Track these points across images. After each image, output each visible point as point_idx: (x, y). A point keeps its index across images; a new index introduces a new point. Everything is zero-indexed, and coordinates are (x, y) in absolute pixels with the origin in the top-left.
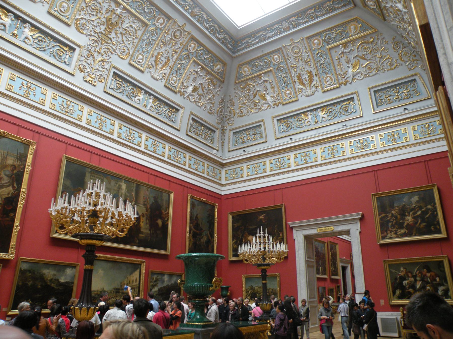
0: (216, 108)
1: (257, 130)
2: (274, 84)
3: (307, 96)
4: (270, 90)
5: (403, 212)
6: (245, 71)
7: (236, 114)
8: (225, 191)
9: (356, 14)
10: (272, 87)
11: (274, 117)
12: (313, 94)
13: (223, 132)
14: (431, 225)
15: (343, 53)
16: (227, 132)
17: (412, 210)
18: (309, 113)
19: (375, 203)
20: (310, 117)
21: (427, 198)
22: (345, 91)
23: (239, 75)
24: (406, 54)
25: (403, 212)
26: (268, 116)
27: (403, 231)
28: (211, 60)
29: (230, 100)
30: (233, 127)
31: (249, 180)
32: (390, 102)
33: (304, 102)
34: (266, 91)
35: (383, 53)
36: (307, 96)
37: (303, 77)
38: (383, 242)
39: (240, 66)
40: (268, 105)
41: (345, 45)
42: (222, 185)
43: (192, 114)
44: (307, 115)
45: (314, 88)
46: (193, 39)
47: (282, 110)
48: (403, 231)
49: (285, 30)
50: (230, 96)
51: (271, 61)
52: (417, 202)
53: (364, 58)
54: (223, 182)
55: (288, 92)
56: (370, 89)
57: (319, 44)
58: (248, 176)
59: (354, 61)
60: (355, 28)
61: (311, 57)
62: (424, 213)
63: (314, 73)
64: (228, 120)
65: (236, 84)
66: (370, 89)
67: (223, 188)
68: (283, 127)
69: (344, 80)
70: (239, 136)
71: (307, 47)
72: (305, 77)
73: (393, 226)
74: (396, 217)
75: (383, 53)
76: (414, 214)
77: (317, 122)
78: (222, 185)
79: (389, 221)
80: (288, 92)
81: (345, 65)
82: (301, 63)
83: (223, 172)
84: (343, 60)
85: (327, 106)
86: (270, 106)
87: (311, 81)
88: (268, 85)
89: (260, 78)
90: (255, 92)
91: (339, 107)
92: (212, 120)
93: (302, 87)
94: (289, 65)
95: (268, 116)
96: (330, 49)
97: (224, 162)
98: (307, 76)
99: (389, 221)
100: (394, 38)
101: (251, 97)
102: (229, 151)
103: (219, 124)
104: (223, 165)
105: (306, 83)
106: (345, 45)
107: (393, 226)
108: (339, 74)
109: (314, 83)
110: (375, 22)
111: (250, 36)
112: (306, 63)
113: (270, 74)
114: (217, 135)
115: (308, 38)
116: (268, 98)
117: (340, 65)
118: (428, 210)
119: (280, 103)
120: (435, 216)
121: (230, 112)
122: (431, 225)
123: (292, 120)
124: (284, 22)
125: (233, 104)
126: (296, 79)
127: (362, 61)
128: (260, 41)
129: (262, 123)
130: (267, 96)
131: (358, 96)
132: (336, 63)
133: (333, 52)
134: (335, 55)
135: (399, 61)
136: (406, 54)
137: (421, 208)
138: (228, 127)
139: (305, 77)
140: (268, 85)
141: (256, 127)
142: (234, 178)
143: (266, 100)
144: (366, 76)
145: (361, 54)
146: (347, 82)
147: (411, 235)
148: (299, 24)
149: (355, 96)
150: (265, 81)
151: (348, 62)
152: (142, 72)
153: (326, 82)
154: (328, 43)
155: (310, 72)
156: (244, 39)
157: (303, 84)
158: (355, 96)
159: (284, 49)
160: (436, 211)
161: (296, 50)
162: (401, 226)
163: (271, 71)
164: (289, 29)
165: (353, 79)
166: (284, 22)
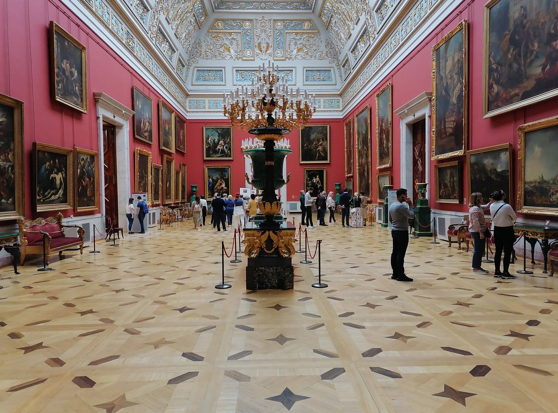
0: (190, 49)
2: (239, 42)
3: (261, 59)
7: (202, 56)
8: (189, 116)
15: (294, 39)
16: (192, 68)
22: (287, 64)
23: (213, 27)
24: (330, 53)
26: (229, 64)
30: (197, 65)
36: (261, 59)
37: (262, 45)
41: (297, 34)
42: (187, 112)
43: (180, 55)
45: (268, 56)
47: (240, 64)
49: (261, 8)
50: (200, 39)
58: (210, 108)
59: (299, 47)
61: (272, 33)
63: (270, 45)
64: (194, 58)
65: (208, 32)
67: (188, 114)
71: (272, 26)
72: (264, 45)
78: (187, 112)
81: (293, 46)
82: (263, 35)
83: (187, 101)
84: (292, 43)
88: (235, 42)
90: (223, 44)
92: (186, 57)
93: (260, 52)
94: (255, 33)
95: (229, 64)
97: (189, 93)
98: (265, 45)
100: (327, 40)
104: (188, 95)
105: (263, 49)
109: (269, 52)
110: (322, 29)
112: (269, 36)
113: (239, 34)
116: (232, 51)
117: (289, 45)
119: (240, 58)
123: (247, 73)
124: (263, 3)
125: (200, 46)
126: (257, 45)
128: (239, 9)
129: (223, 69)
130: (231, 49)
132: (288, 43)
133: (288, 35)
134: (289, 38)
138: (194, 65)
139: (264, 45)
140: (235, 42)
141: (219, 71)
143: (230, 52)
145: (304, 43)
146: (290, 58)
149: (294, 69)
150: (233, 39)
152: (169, 23)
153: (277, 53)
155: (268, 44)
158: (294, 69)
159: (255, 21)
164: (265, 8)
165: (295, 58)
166: (263, 3)
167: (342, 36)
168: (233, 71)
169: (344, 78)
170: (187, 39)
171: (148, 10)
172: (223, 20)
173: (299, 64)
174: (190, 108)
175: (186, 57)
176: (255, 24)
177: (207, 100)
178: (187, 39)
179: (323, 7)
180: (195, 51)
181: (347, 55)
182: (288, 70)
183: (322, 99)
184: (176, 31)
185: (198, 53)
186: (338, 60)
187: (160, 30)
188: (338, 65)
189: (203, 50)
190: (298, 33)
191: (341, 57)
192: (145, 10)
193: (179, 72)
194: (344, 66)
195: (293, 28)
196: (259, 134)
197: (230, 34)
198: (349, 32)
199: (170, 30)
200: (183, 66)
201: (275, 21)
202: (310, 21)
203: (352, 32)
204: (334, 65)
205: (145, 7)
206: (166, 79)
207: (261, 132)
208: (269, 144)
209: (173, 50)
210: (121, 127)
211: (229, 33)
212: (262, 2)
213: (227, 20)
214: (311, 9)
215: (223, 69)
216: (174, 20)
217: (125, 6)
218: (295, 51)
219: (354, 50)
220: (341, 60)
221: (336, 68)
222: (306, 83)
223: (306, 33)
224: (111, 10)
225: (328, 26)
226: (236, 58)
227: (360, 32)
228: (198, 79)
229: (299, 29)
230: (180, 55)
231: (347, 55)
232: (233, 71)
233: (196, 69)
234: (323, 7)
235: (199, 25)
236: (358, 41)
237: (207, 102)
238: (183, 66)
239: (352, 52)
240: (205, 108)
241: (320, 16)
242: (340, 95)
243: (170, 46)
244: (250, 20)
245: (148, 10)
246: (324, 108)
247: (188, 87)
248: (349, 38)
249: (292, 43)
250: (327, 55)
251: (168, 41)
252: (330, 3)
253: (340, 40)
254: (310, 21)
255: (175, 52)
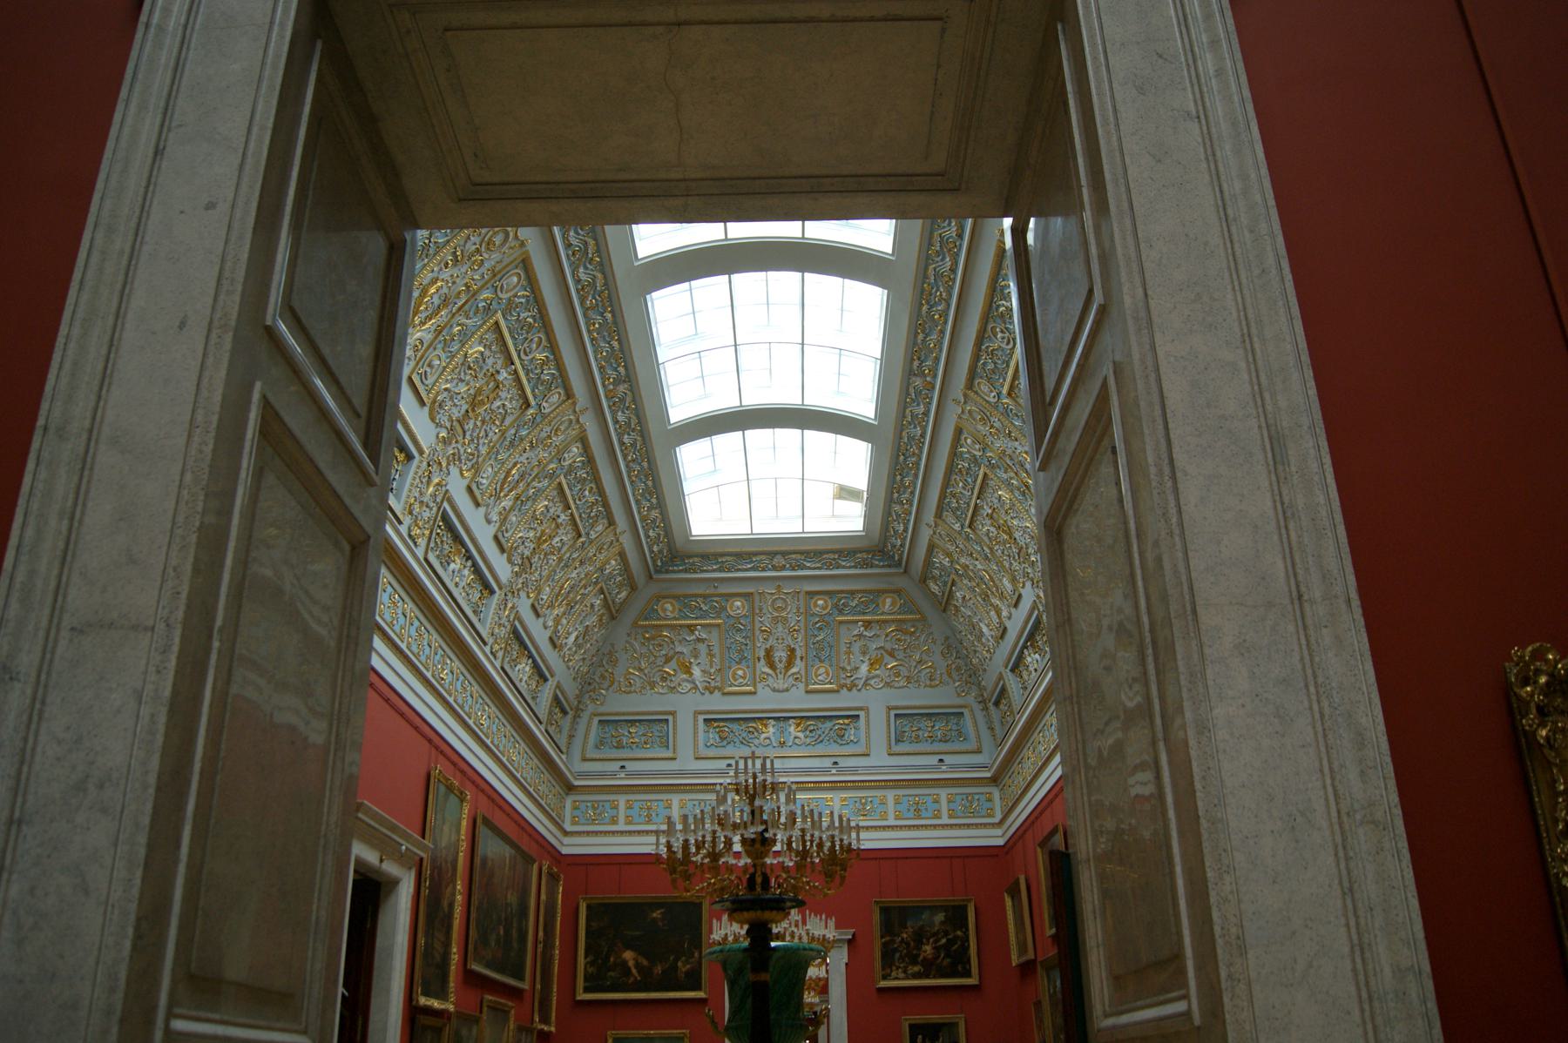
1: (657, 727)
2: (716, 650)
3: (774, 690)
4: (703, 658)
5: (920, 937)
6: (665, 610)
8: (570, 847)
9: (901, 582)
10: (711, 655)
11: (701, 713)
12: (787, 690)
13: (578, 711)
14: (958, 964)
15: (860, 636)
16: (585, 716)
17: (935, 934)
18: (772, 722)
19: (876, 917)
20: (771, 730)
21: (957, 916)
22: (845, 700)
23: (648, 613)
24: (958, 669)
25: (920, 937)
26: (687, 705)
27: (916, 969)
28: (620, 586)
29: (610, 653)
30: (602, 709)
31: (630, 833)
32: (918, 740)
33: (765, 700)
34: (696, 657)
35: (925, 657)
36: (774, 690)
38: (883, 984)
39: (659, 598)
40: (689, 686)
41: (868, 624)
42: (566, 833)
44: (766, 726)
46: (622, 555)
47: (717, 703)
48: (916, 969)
49: (775, 568)
51: (724, 609)
52: (942, 923)
53: (892, 655)
54: (568, 827)
55: (740, 673)
56: (889, 709)
57: (824, 608)
58: (630, 823)
60: (893, 604)
62: (950, 942)
63: (799, 653)
65: (635, 625)
66: (889, 709)
67: (567, 840)
68: (713, 736)
69: (848, 681)
70: (610, 730)
72: (780, 655)
73: (902, 958)
74: (908, 944)
75: (925, 657)
76: (936, 941)
77: (782, 744)
78: (566, 833)
79: (895, 950)
80: (740, 673)
81: (856, 657)
84: (856, 648)
85: (808, 718)
86: (696, 687)
87: (790, 663)
88: (702, 647)
89: (692, 632)
91: (829, 724)
94: (758, 625)
95: (687, 705)
96: (841, 622)
97: (576, 783)
98: (784, 654)
99: (895, 950)
100: (947, 638)
101: (660, 661)
102: (585, 760)
103: (579, 698)
104: (570, 788)
105: (780, 666)
106: (868, 624)
107: (902, 958)
108: (843, 669)
109: (794, 670)
111: (705, 557)
112: (792, 631)
113: (715, 633)
114: (566, 723)
115: (809, 593)
116: (696, 672)
117: (849, 653)
118: (956, 937)
120: (965, 948)
121: (603, 677)
122: (958, 964)
123: (735, 727)
125: (614, 663)
126: (762, 654)
127: (887, 657)
129: (670, 718)
131: (868, 716)
133: (843, 629)
134: (846, 635)
135: (945, 677)
136: (958, 669)
137: (946, 933)
138: (591, 708)
139: (780, 655)
140: (702, 647)
141: (658, 725)
142: (593, 822)
144: (888, 684)
145: (888, 646)
147: (927, 977)
148: (804, 568)
149: (862, 714)
150: (698, 640)
151: (864, 653)
152: (538, 615)
154: (841, 612)
155: (793, 650)
156: (690, 557)
157: (772, 666)
158: (862, 714)
159: (757, 598)
160: (968, 940)
161: (779, 604)
162: (914, 960)
163: (718, 625)
164: (783, 568)
165: (866, 684)
167: (985, 629)
168: (695, 720)
169: (999, 732)
170: (579, 646)
171: (492, 592)
172: (676, 597)
173: (876, 702)
174: (574, 823)
175: (571, 689)
176: (757, 604)
177: (622, 800)
178: (579, 646)
179: (928, 563)
180: (598, 672)
181: (1001, 677)
182: (848, 717)
183: (943, 793)
184: (556, 631)
185: (603, 677)
186: (981, 689)
187: (515, 632)
188: (983, 702)
189: (619, 672)
190: (870, 622)
191: (989, 681)
192: (486, 593)
193: (551, 730)
194: (997, 704)
195: (854, 611)
196: (735, 910)
197: (691, 629)
198: (1001, 623)
199: (539, 632)
200: (564, 712)
201: (811, 594)
202: (898, 592)
203: (1008, 624)
204: (971, 699)
205: (486, 586)
206: (517, 753)
207: (737, 907)
208: (760, 933)
209: (540, 675)
210: (394, 883)
211: (689, 626)
212: (775, 553)
213: (686, 596)
214: (899, 564)
215: (670, 718)
216: (551, 606)
217: (447, 602)
218: (864, 668)
219: (1017, 666)
220: (989, 689)
221: (977, 708)
222: (896, 749)
223: (893, 621)
224: (409, 606)
225: (945, 604)
226: (706, 688)
227: (1026, 622)
228: (600, 744)
229: (873, 613)
230: (558, 686)
231: (1001, 677)
232: (695, 720)
233: (596, 720)
234: (928, 563)
235: (612, 613)
236: (1025, 647)
237: (622, 806)
238: (564, 712)
239: (1012, 670)
240: (614, 821)
241: (924, 580)
242: (995, 780)
243: (536, 666)
244: (747, 596)
245: (492, 592)
246: (950, 817)
247: (572, 766)
248: (1002, 637)
249: (856, 648)
250: (950, 675)
251: (530, 656)
252: (949, 555)
253: (979, 640)
254: (898, 592)
255: (546, 680)
